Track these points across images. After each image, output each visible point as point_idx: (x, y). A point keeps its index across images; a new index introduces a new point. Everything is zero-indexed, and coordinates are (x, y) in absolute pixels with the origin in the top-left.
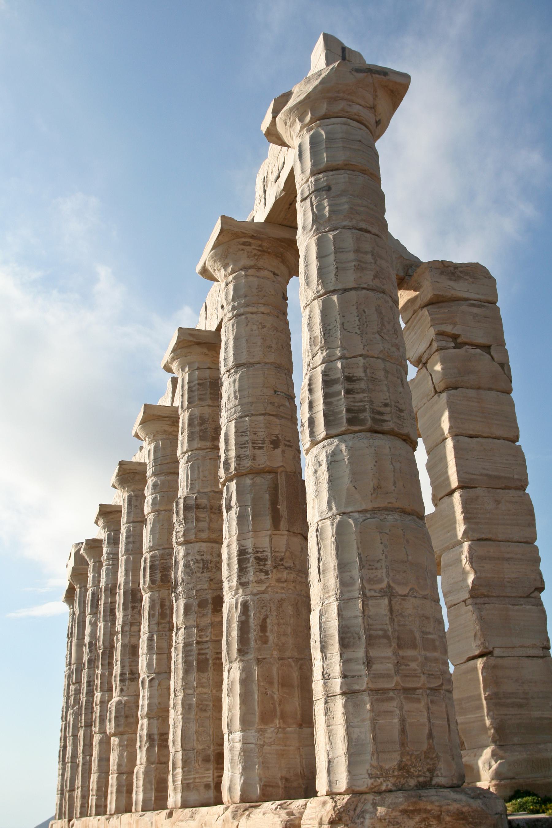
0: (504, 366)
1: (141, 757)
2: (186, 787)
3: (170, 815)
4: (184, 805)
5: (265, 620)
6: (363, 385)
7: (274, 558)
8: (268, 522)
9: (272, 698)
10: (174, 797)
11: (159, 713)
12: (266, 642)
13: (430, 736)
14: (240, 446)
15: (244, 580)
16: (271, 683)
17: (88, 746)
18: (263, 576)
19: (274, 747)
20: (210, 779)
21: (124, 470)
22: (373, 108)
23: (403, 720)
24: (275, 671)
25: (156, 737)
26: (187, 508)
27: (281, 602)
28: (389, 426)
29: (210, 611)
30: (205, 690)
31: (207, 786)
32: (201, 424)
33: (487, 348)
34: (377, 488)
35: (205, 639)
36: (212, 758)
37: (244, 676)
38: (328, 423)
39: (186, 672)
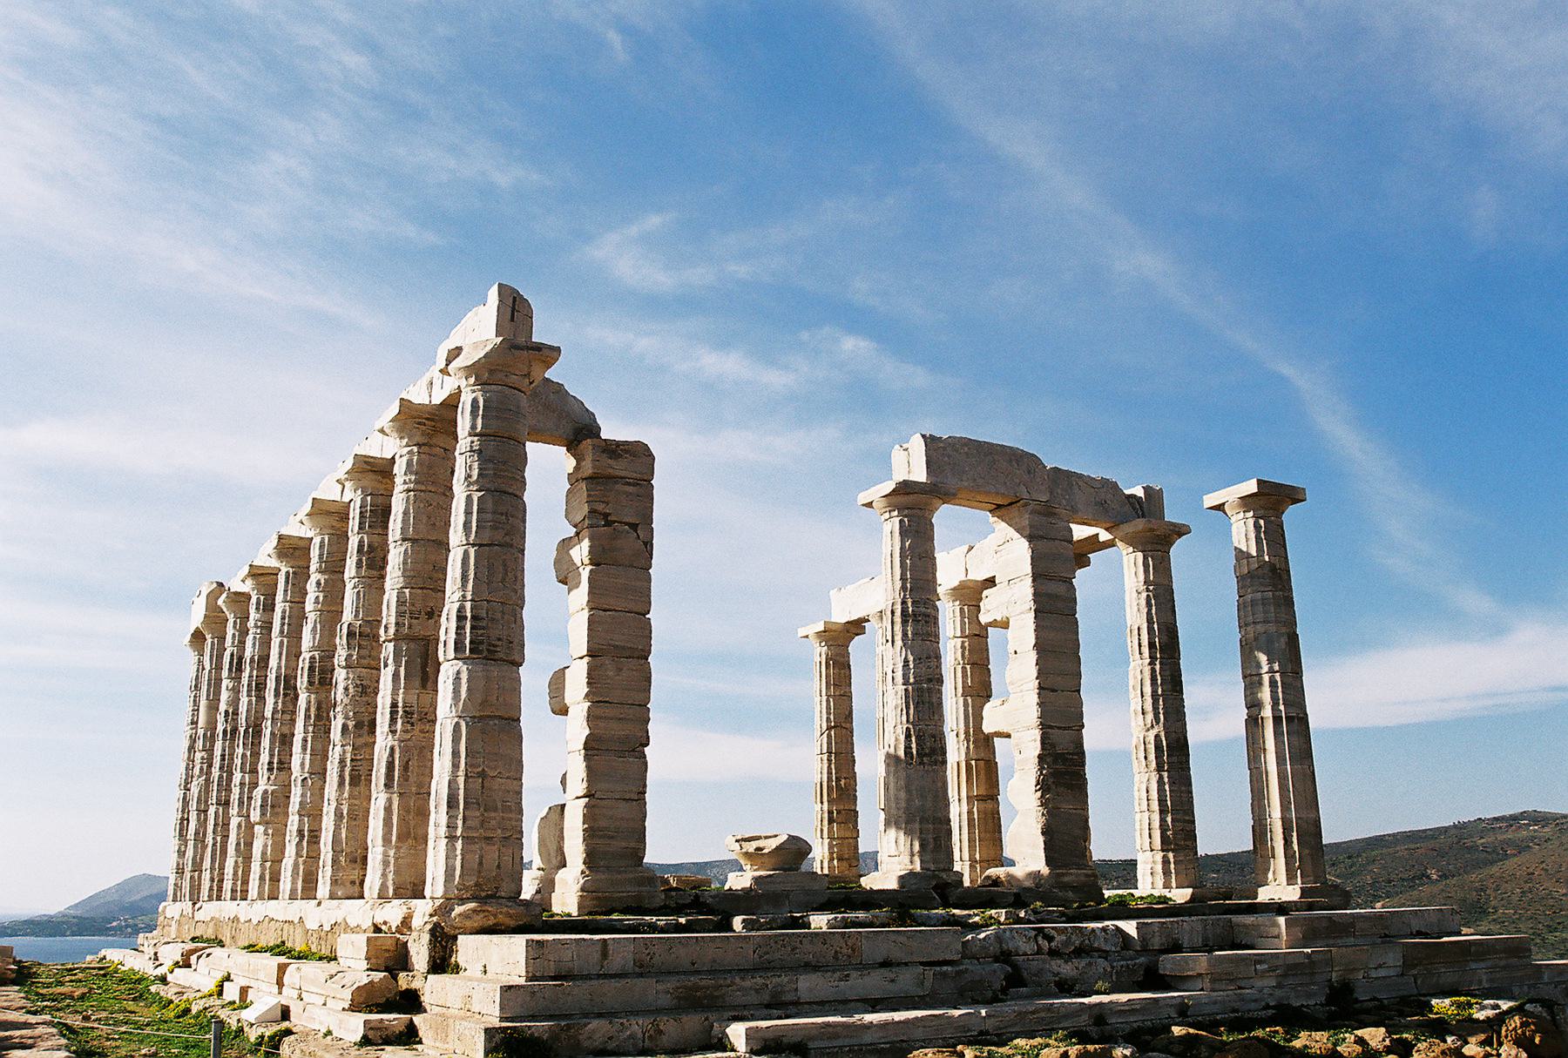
0: (648, 545)
1: (291, 850)
2: (334, 882)
3: (319, 904)
4: (332, 897)
6: (484, 624)
7: (420, 713)
8: (417, 683)
10: (323, 889)
11: (312, 812)
13: (499, 867)
14: (400, 614)
17: (223, 826)
22: (528, 375)
23: (481, 857)
26: (350, 634)
28: (501, 655)
31: (353, 883)
32: (369, 552)
33: (634, 527)
34: (484, 703)
38: (456, 650)
39: (341, 783)
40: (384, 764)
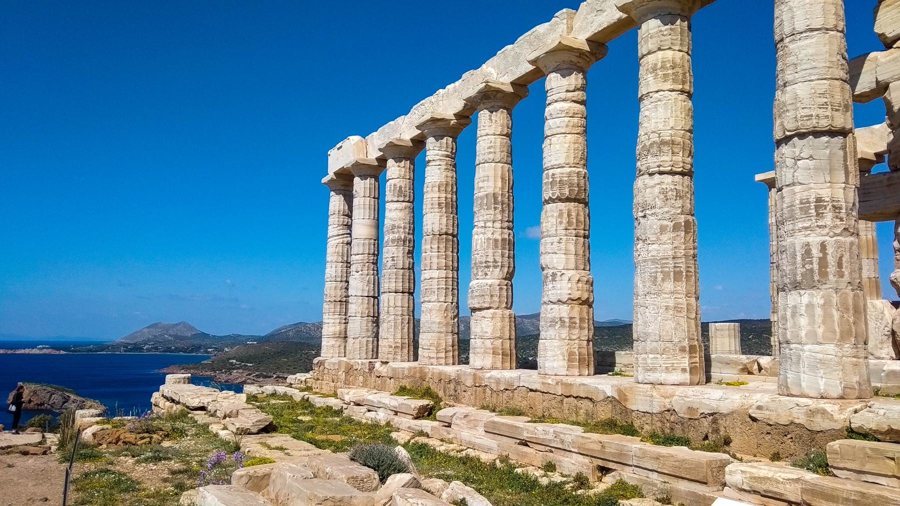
5: (841, 258)
9: (848, 320)
12: (842, 276)
15: (820, 223)
16: (848, 309)
18: (838, 222)
19: (849, 359)
20: (687, 364)
21: (490, 87)
24: (850, 302)
27: (852, 244)
29: (683, 234)
30: (679, 296)
35: (679, 255)
36: (688, 349)
37: (822, 302)
40: (815, 261)
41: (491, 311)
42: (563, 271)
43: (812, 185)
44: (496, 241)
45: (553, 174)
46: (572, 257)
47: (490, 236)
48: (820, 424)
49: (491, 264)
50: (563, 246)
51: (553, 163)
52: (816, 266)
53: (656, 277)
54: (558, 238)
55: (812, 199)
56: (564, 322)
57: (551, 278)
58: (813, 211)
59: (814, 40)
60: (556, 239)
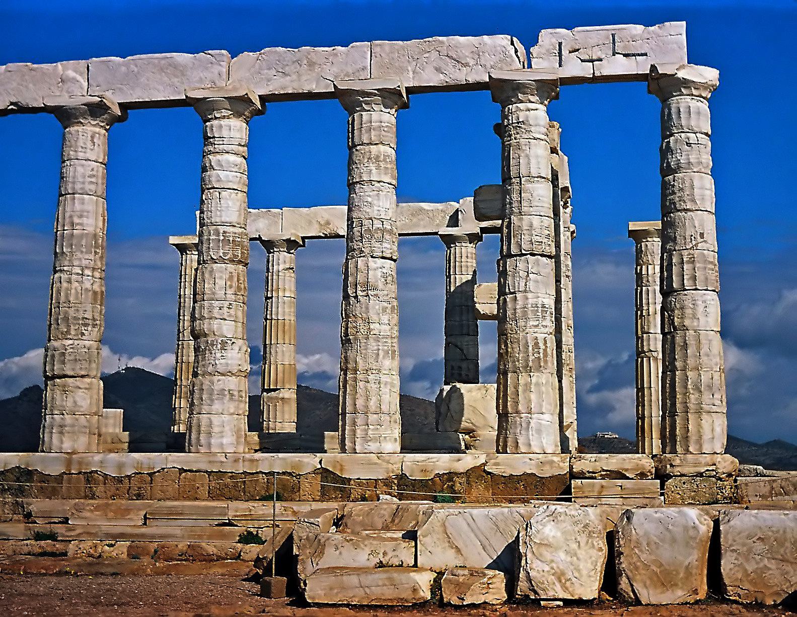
25: (236, 393)
40: (541, 351)
41: (87, 380)
42: (233, 340)
43: (540, 295)
44: (95, 293)
45: (224, 232)
46: (240, 325)
47: (87, 285)
48: (547, 472)
49: (90, 322)
50: (232, 312)
51: (223, 219)
52: (541, 355)
53: (378, 355)
54: (228, 303)
55: (539, 306)
56: (232, 395)
57: (219, 346)
58: (540, 314)
59: (542, 185)
60: (226, 304)
